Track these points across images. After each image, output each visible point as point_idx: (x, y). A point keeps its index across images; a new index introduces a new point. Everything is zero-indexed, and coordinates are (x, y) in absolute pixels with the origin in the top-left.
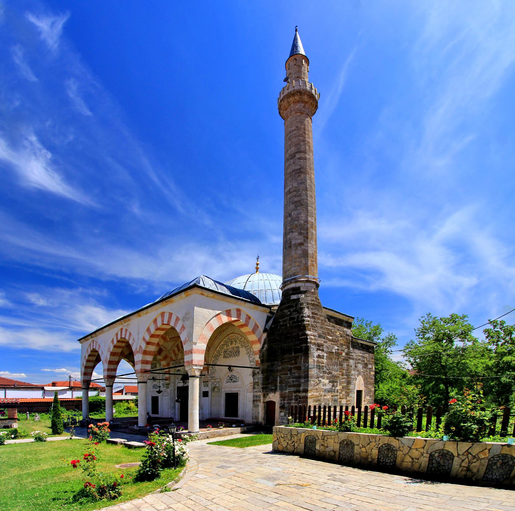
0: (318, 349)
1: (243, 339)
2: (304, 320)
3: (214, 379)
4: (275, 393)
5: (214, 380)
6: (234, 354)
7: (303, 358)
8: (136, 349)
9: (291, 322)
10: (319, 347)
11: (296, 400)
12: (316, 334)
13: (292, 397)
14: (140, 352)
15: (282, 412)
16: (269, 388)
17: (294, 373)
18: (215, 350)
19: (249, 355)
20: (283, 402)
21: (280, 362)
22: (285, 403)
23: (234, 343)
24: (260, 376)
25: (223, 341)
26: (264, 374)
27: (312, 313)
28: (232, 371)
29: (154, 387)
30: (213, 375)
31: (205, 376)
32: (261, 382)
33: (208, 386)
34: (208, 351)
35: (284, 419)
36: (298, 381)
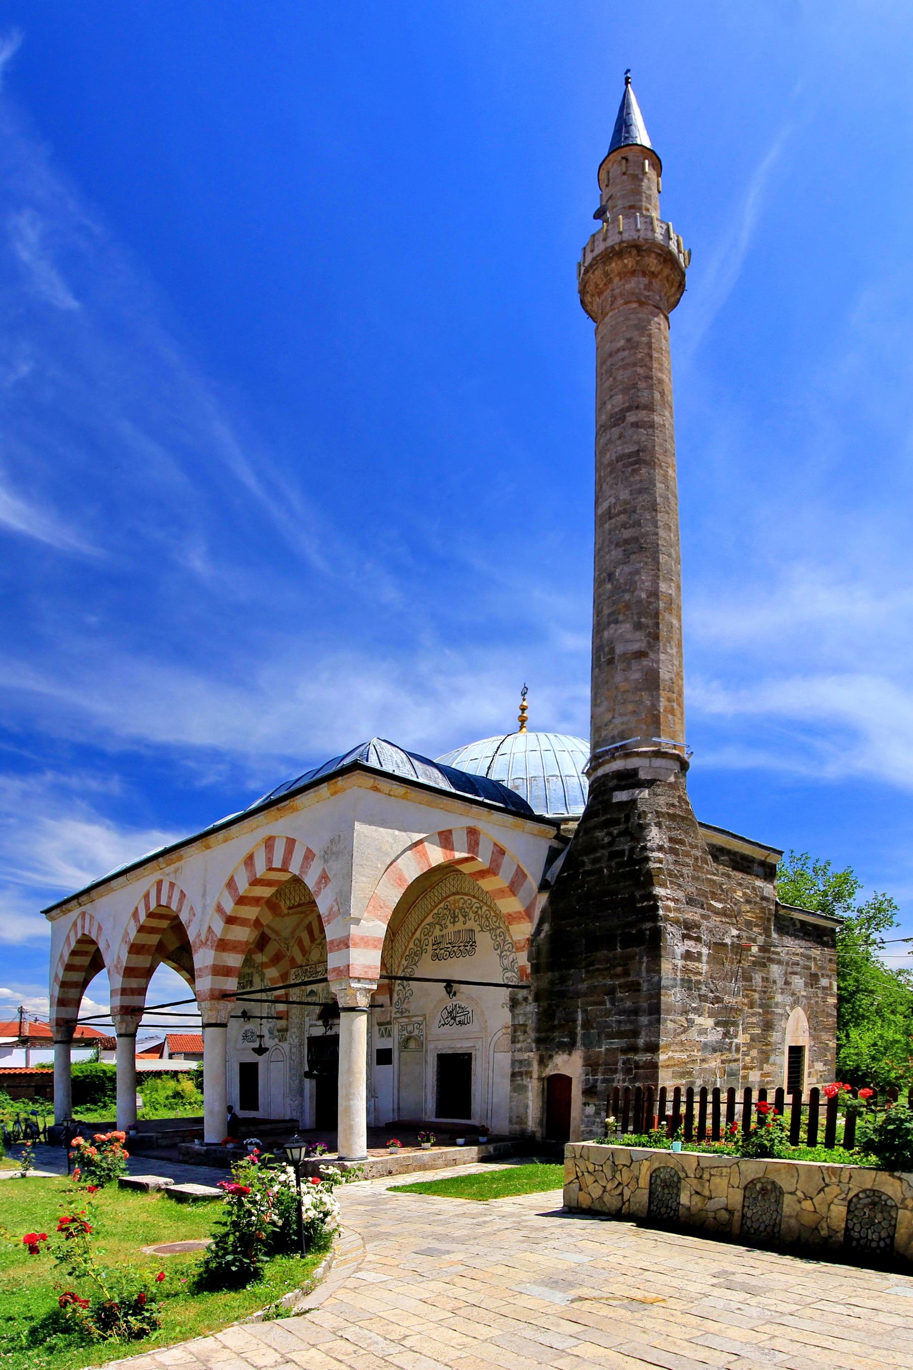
0: (684, 937)
1: (485, 908)
2: (647, 859)
3: (408, 1017)
4: (570, 1054)
5: (406, 1020)
6: (462, 948)
7: (645, 959)
8: (199, 935)
9: (613, 864)
10: (689, 930)
11: (627, 1071)
12: (680, 895)
13: (616, 1064)
14: (209, 943)
15: (589, 1104)
16: (554, 1039)
17: (622, 1000)
18: (411, 938)
19: (502, 952)
20: (591, 1077)
21: (583, 970)
22: (597, 1079)
23: (462, 919)
24: (531, 1008)
25: (431, 915)
26: (542, 1004)
27: (671, 840)
28: (455, 994)
29: (245, 1037)
30: (405, 1006)
31: (383, 1009)
32: (534, 1025)
33: (390, 1036)
34: (392, 941)
35: (594, 1122)
36: (631, 1022)
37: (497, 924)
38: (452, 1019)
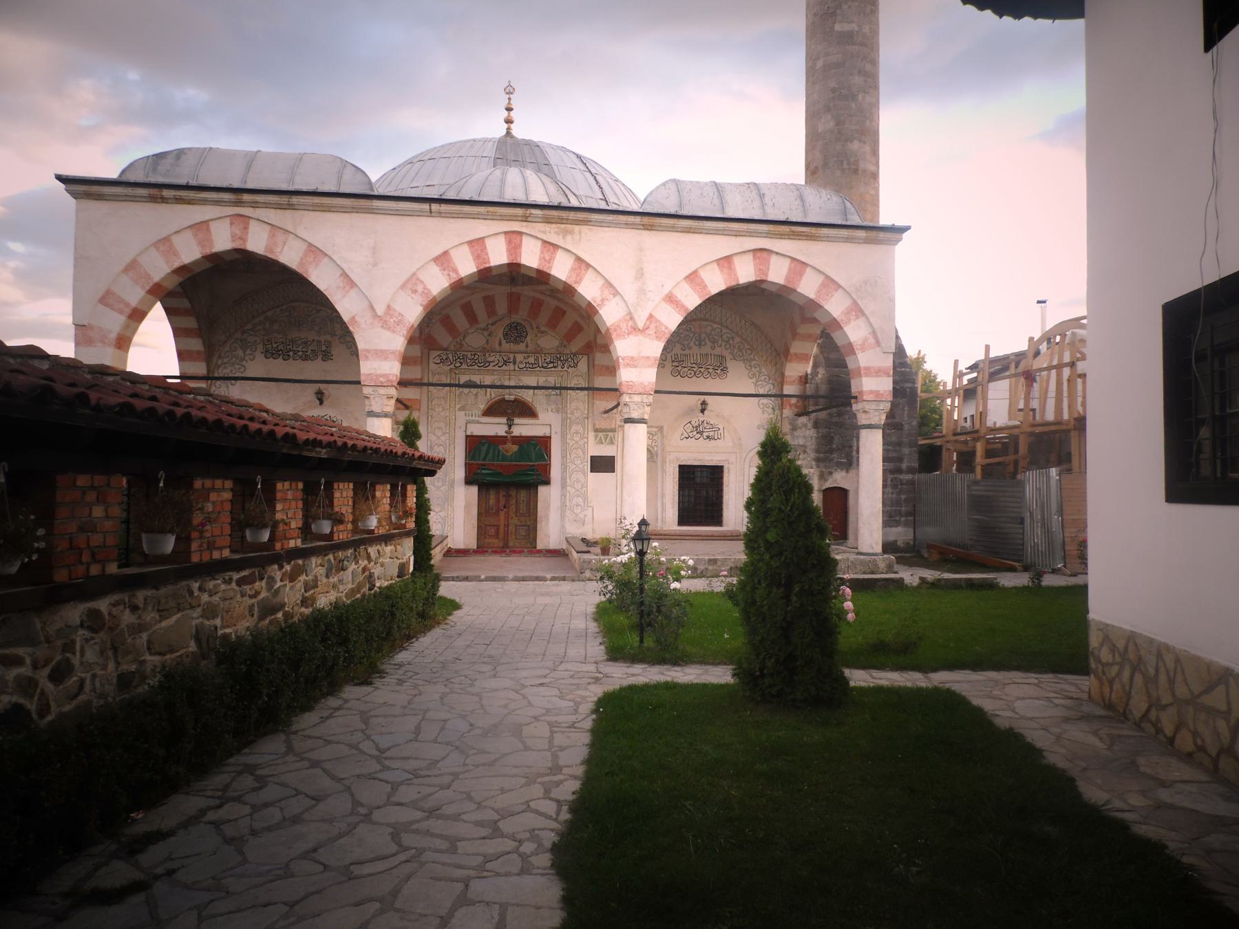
4: (847, 472)
16: (831, 460)
19: (757, 382)
24: (811, 433)
32: (813, 447)
33: (612, 443)
36: (896, 451)
37: (752, 357)
38: (698, 433)
